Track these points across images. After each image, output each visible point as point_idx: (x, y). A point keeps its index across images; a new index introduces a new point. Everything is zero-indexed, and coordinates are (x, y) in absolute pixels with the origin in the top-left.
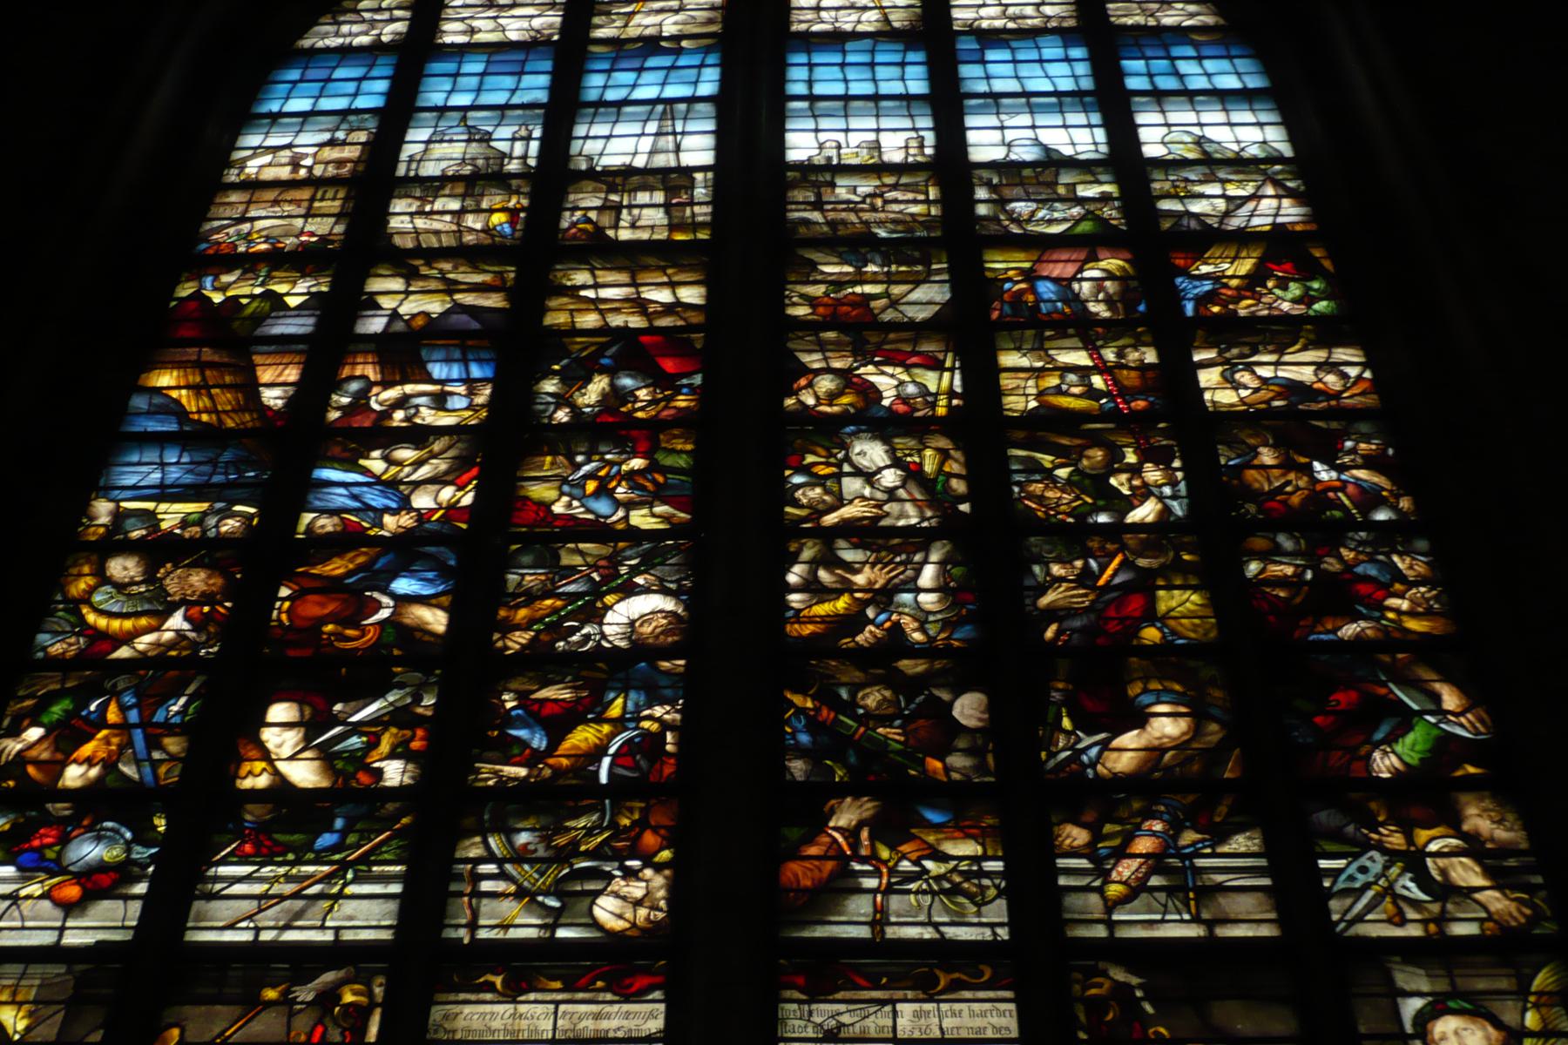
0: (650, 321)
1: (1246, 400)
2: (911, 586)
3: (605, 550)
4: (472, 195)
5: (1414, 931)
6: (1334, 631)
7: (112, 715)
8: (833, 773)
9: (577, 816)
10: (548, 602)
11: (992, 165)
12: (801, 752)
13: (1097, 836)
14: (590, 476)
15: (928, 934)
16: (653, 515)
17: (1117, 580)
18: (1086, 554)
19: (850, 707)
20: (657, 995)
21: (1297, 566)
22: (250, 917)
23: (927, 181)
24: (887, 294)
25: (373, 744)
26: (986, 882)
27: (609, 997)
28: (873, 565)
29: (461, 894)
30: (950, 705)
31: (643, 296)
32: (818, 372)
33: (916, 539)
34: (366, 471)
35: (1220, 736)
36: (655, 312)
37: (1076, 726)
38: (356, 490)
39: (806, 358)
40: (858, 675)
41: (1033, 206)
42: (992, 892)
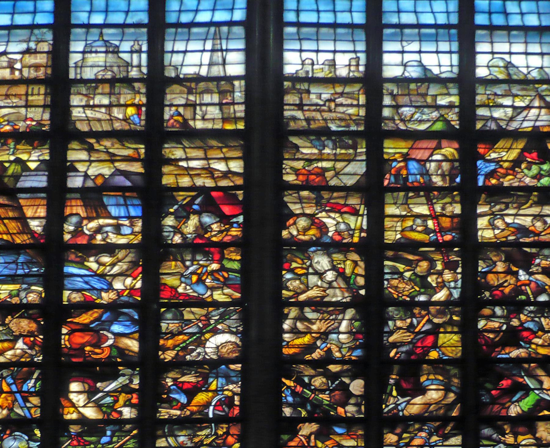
0: (216, 182)
1: (497, 236)
3: (203, 311)
4: (114, 94)
8: (301, 413)
9: (201, 429)
10: (181, 337)
11: (394, 80)
12: (289, 405)
13: (400, 438)
14: (193, 273)
16: (224, 294)
17: (424, 329)
18: (413, 316)
19: (308, 386)
21: (501, 323)
23: (359, 91)
24: (334, 168)
28: (321, 320)
30: (348, 385)
31: (211, 166)
32: (298, 216)
34: (89, 269)
35: (454, 399)
36: (218, 177)
37: (398, 395)
38: (86, 279)
39: (292, 207)
40: (312, 372)
41: (413, 110)
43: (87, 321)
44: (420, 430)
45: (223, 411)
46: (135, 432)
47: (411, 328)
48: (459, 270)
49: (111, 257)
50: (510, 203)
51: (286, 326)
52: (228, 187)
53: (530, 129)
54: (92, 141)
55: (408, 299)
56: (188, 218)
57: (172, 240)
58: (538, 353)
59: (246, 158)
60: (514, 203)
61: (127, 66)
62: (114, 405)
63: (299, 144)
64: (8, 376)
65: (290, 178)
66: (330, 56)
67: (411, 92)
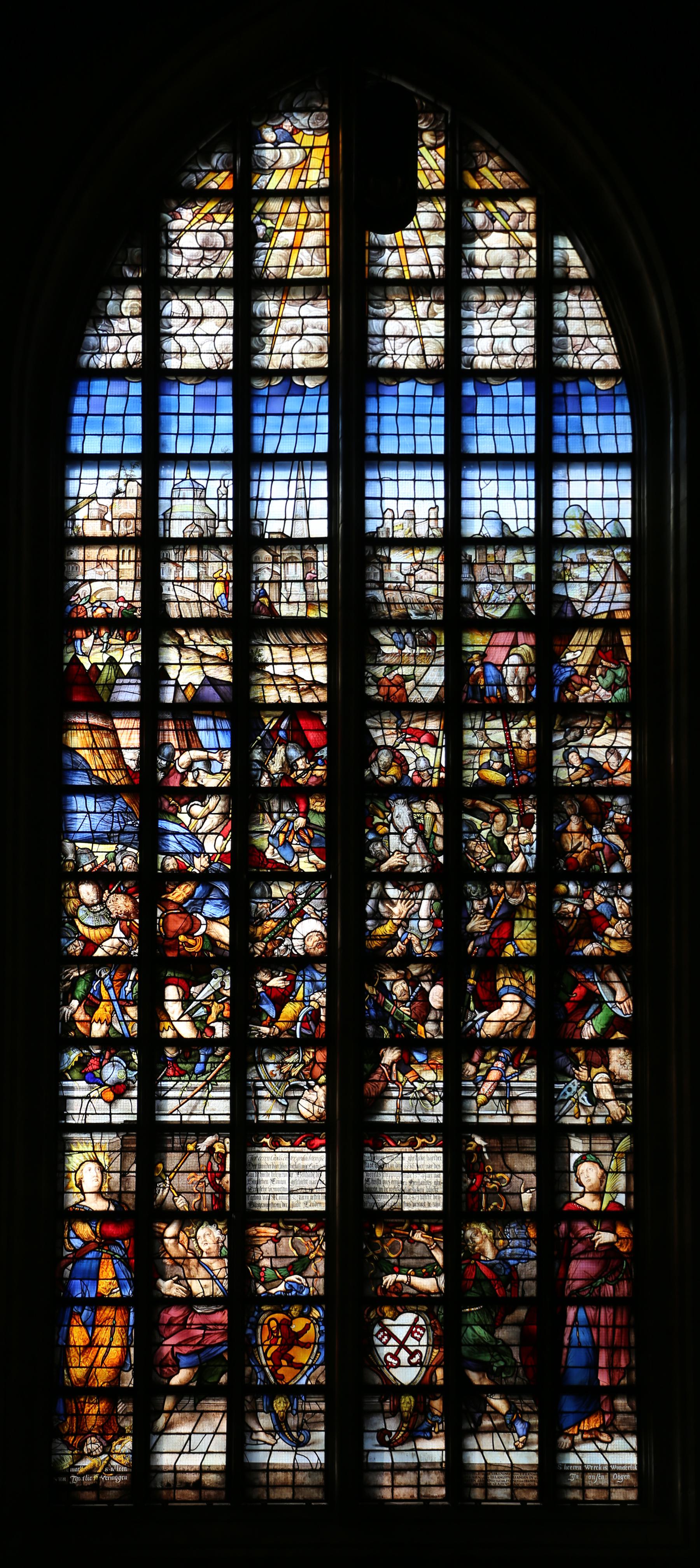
0: (301, 697)
2: (415, 917)
4: (202, 562)
5: (582, 1121)
6: (582, 950)
7: (105, 995)
9: (289, 1056)
10: (269, 923)
13: (478, 1070)
14: (279, 832)
15: (414, 1119)
16: (310, 862)
17: (500, 914)
18: (490, 894)
19: (389, 994)
20: (323, 1149)
21: (574, 905)
22: (177, 1109)
25: (209, 1012)
26: (436, 1093)
27: (306, 1149)
28: (402, 900)
29: (251, 1097)
30: (428, 994)
31: (297, 673)
32: (381, 748)
33: (420, 880)
34: (181, 824)
35: (528, 1014)
36: (303, 690)
37: (475, 1008)
41: (489, 586)
42: (438, 1099)
43: (180, 899)
44: (497, 1058)
45: (310, 1029)
46: (227, 1057)
47: (488, 910)
48: (534, 829)
49: (202, 806)
50: (585, 727)
51: (368, 909)
52: (313, 703)
53: (604, 616)
54: (182, 633)
55: (485, 870)
56: (275, 751)
57: (259, 781)
58: (610, 949)
59: (330, 663)
60: (589, 728)
61: (214, 519)
62: (207, 1019)
63: (382, 641)
64: (106, 976)
65: (372, 691)
66: (409, 505)
67: (489, 560)
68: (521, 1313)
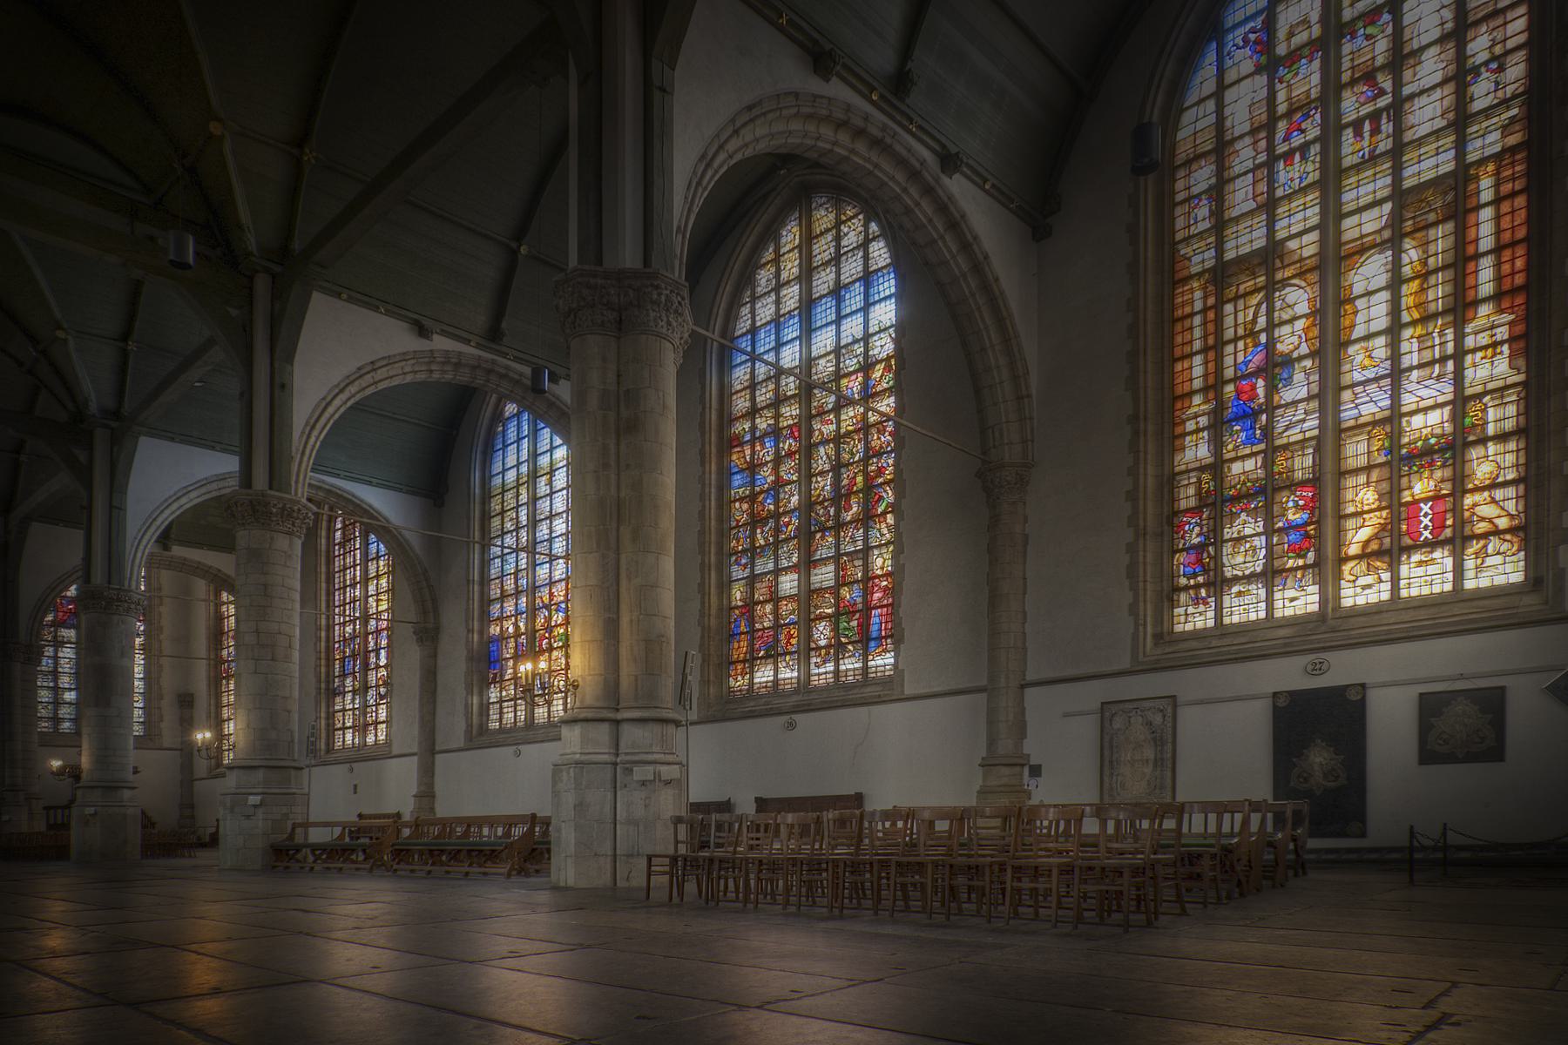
68: (857, 616)
